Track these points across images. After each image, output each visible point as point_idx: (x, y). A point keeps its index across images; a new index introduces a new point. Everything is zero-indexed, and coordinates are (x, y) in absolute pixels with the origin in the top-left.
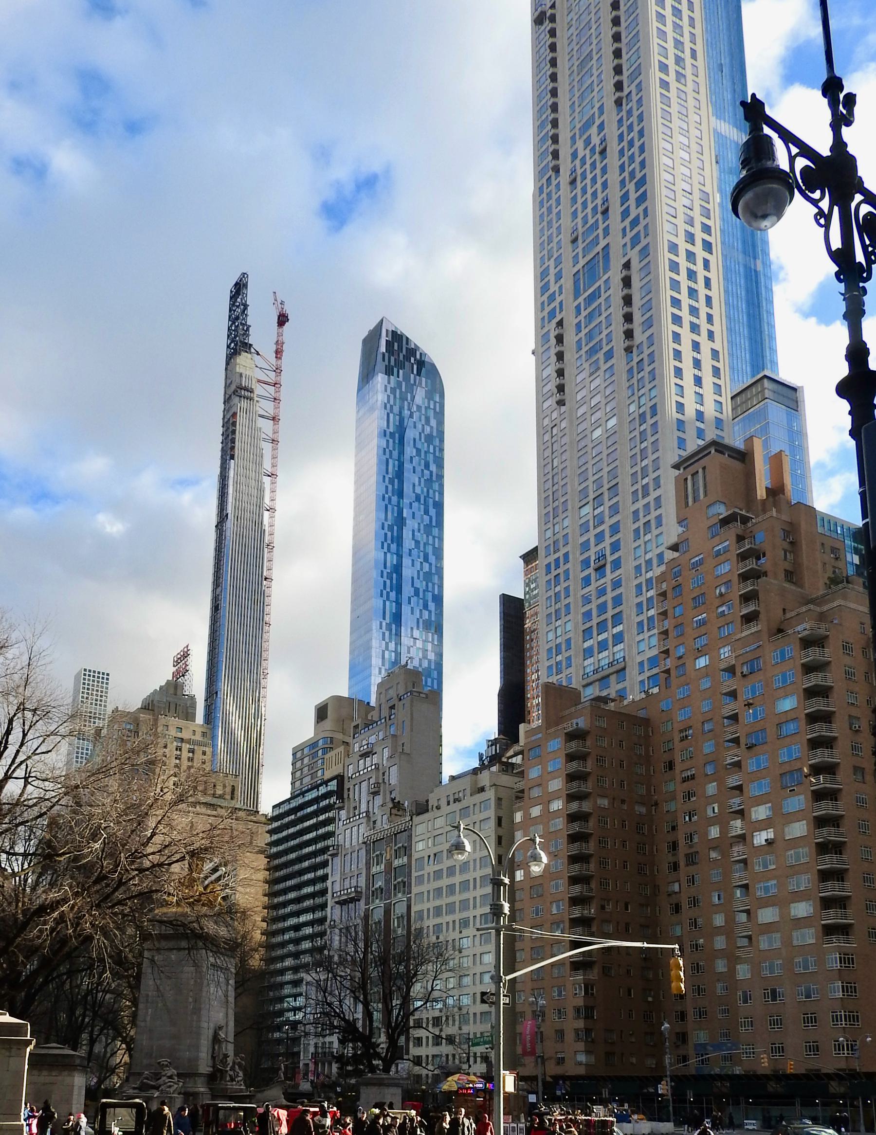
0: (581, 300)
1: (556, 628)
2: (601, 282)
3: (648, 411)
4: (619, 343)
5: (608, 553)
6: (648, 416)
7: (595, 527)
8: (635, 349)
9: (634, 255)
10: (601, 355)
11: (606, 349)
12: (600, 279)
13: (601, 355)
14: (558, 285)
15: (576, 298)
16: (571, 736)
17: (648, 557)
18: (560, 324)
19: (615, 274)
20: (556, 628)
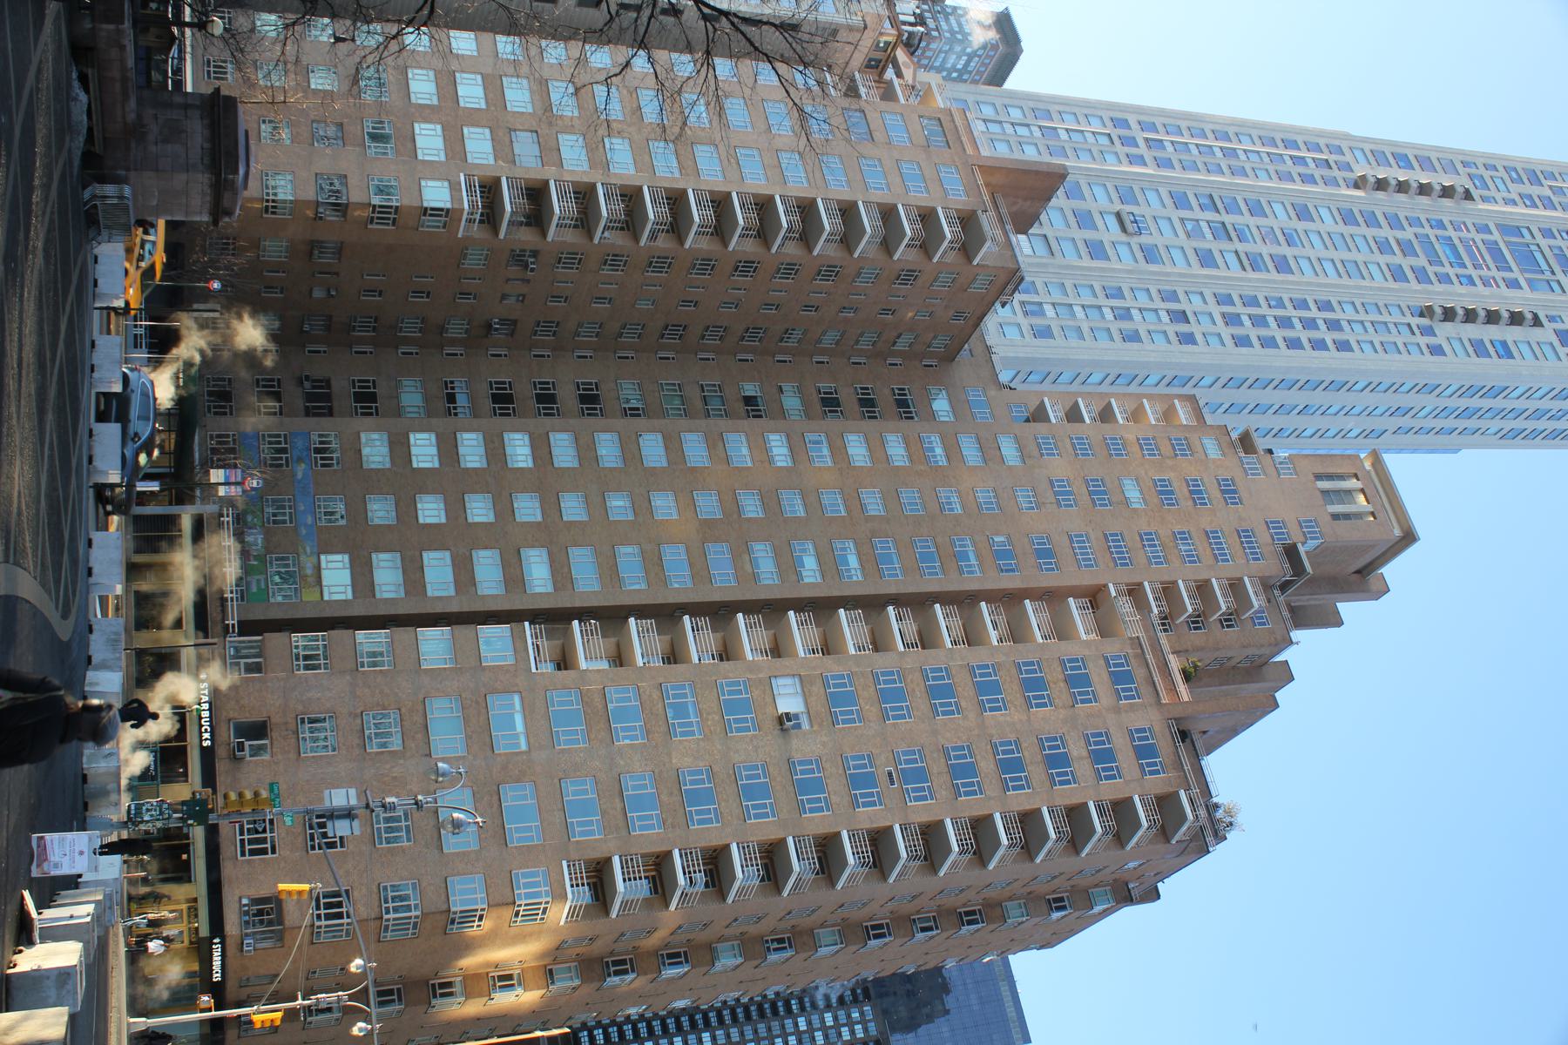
0: (1496, 236)
1: (1028, 125)
2: (1516, 274)
3: (1345, 337)
4: (1440, 295)
5: (1144, 239)
6: (1337, 336)
7: (1182, 220)
8: (1425, 321)
9: (1547, 334)
10: (1422, 261)
11: (1430, 270)
12: (1522, 271)
13: (1422, 261)
14: (1517, 199)
15: (1500, 227)
16: (967, 221)
17: (1135, 312)
18: (1468, 196)
19: (1522, 299)
20: (1028, 125)
